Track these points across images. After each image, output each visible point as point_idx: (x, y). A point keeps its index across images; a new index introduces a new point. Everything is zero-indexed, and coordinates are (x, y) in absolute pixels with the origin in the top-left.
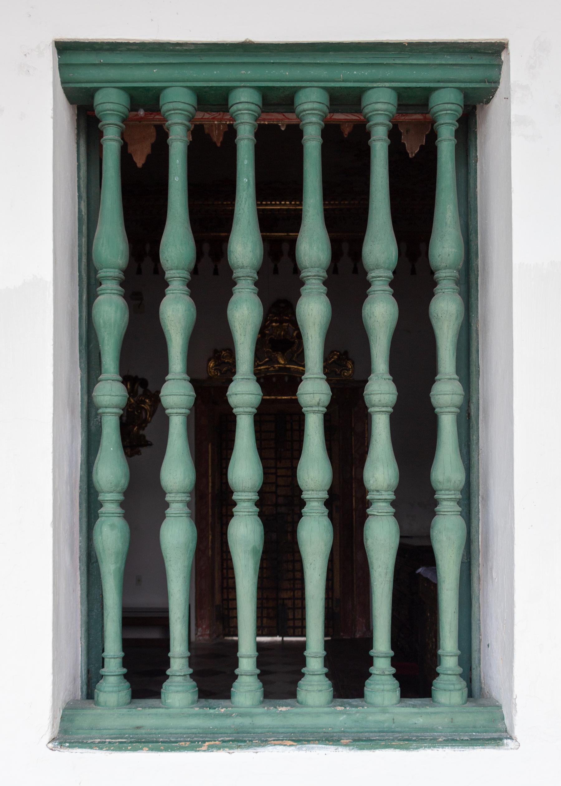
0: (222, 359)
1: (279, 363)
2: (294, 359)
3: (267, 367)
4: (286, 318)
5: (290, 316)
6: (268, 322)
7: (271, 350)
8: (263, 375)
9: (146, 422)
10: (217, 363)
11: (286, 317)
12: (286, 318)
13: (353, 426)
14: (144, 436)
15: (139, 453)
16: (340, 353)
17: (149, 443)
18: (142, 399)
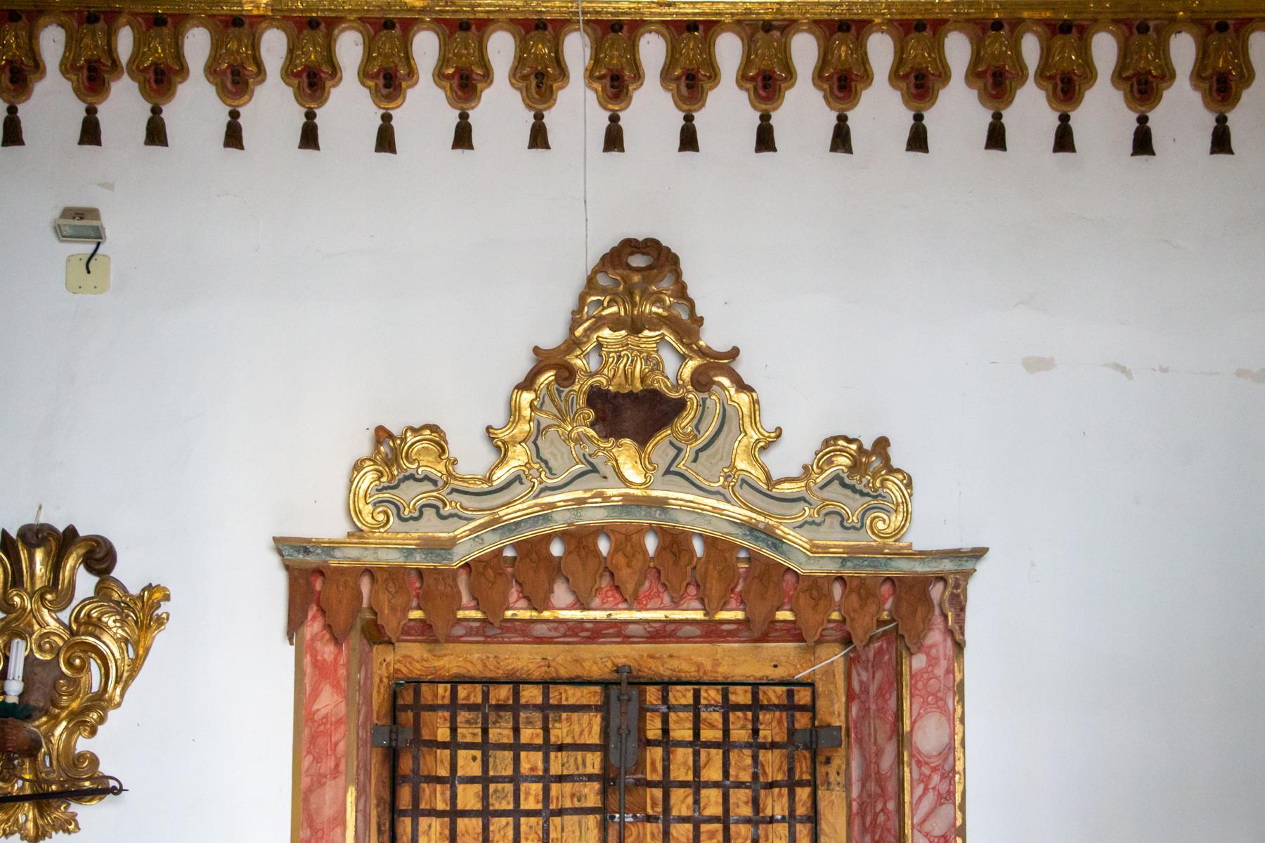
0: (405, 464)
1: (626, 482)
2: (681, 466)
3: (580, 494)
4: (654, 309)
5: (668, 300)
6: (586, 325)
7: (591, 432)
8: (563, 527)
9: (100, 703)
10: (384, 479)
11: (653, 304)
12: (654, 309)
13: (907, 728)
14: (94, 761)
15: (71, 827)
16: (860, 448)
17: (112, 783)
18: (89, 615)
